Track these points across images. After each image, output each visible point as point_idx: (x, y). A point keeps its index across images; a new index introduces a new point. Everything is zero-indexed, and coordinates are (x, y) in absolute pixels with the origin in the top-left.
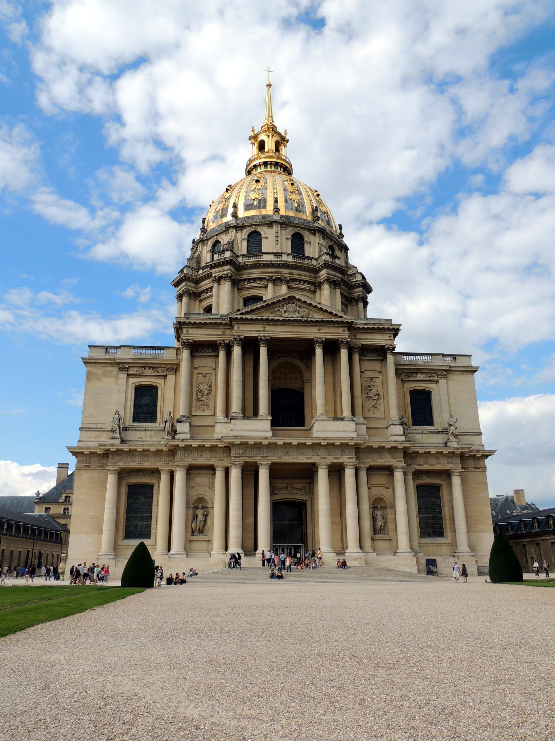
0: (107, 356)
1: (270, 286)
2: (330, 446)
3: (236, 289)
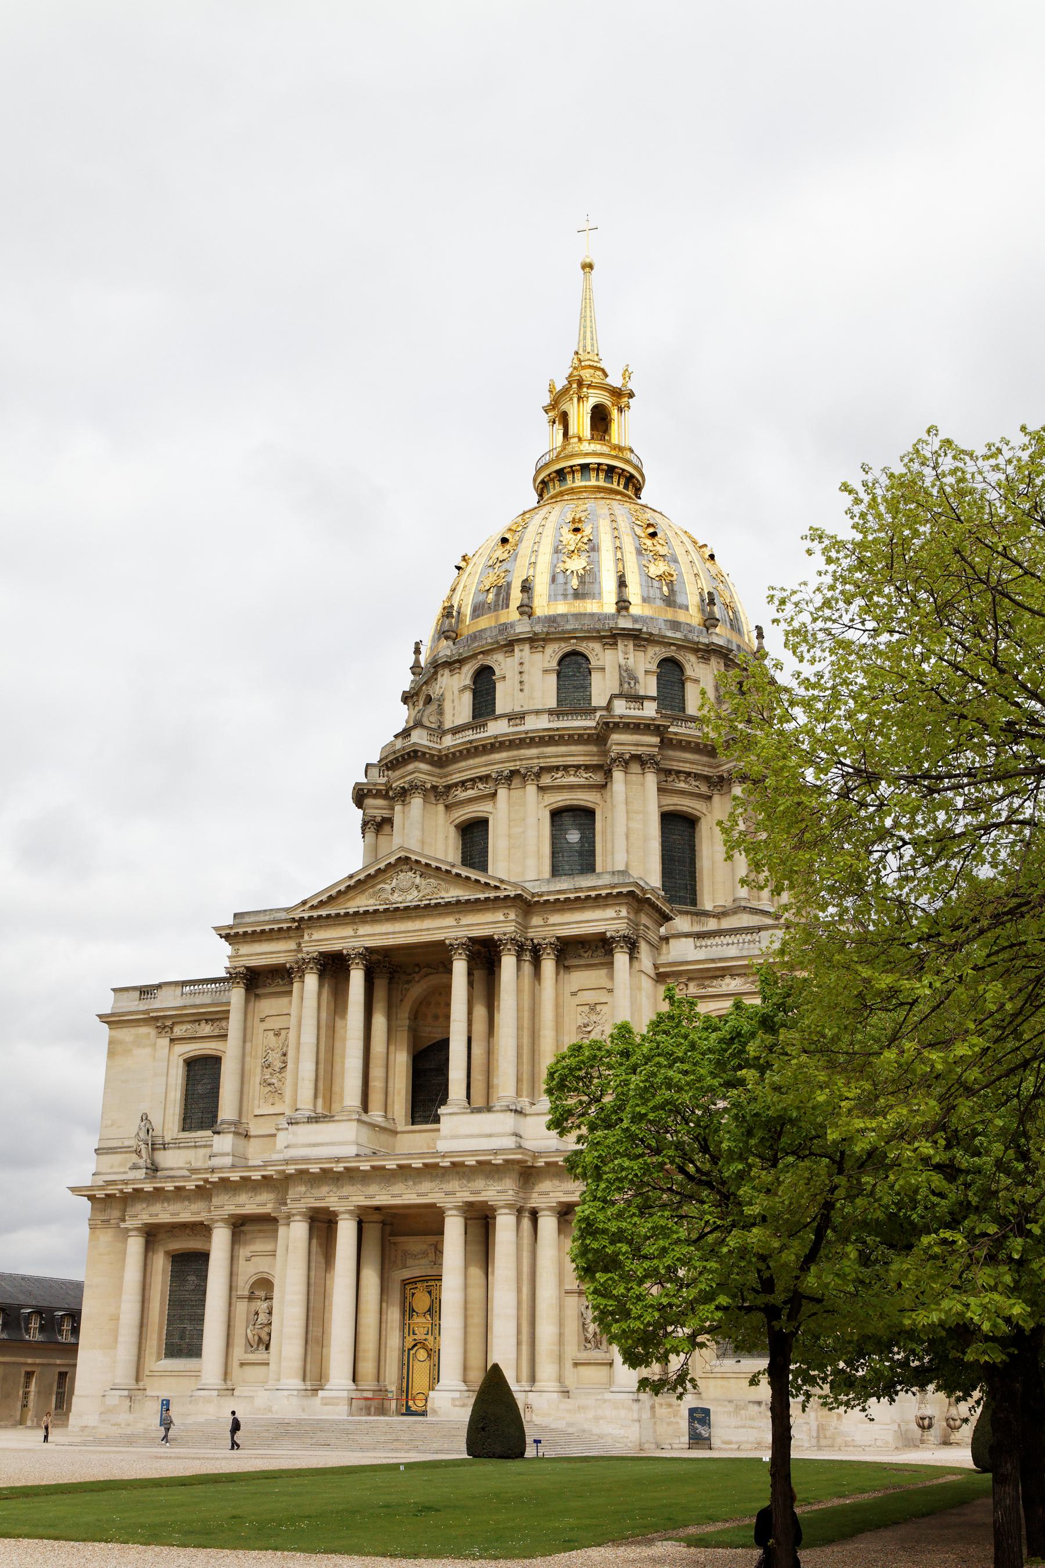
0: (143, 1006)
1: (502, 793)
2: (458, 1170)
3: (441, 808)
